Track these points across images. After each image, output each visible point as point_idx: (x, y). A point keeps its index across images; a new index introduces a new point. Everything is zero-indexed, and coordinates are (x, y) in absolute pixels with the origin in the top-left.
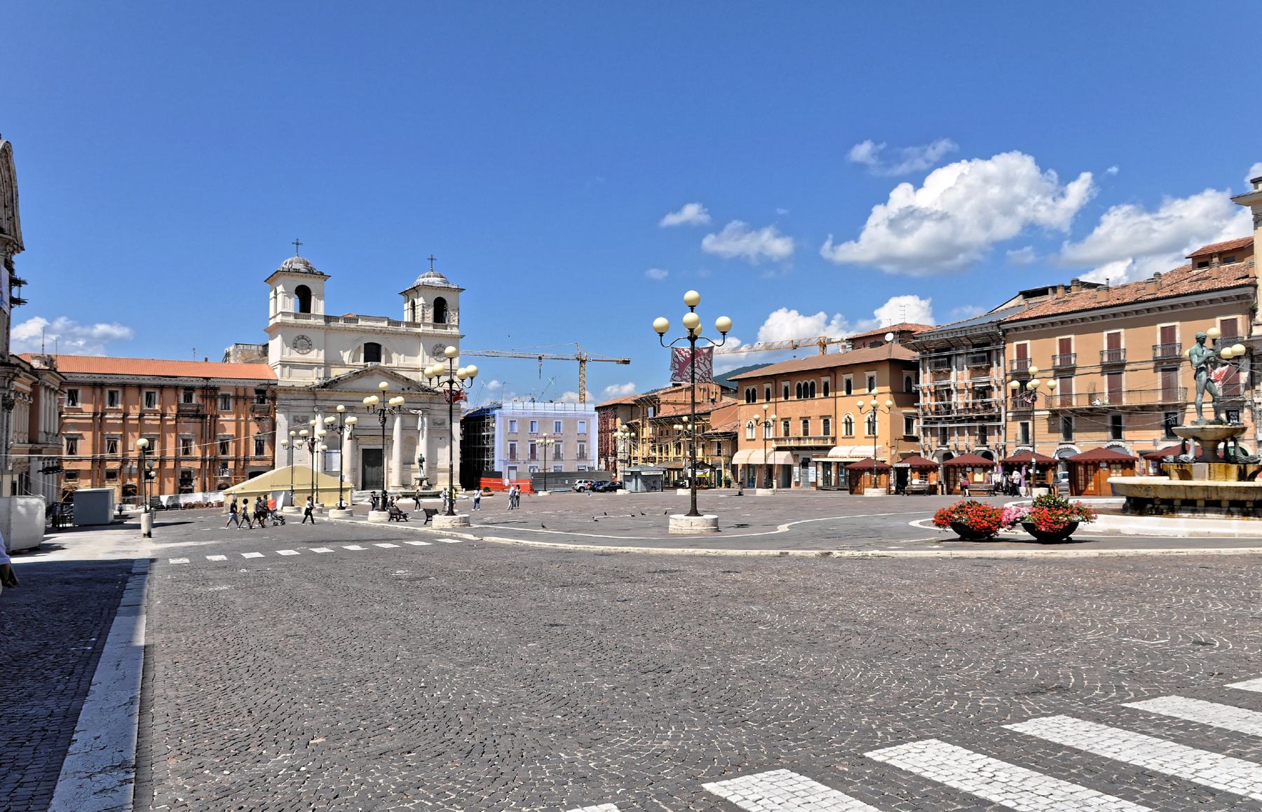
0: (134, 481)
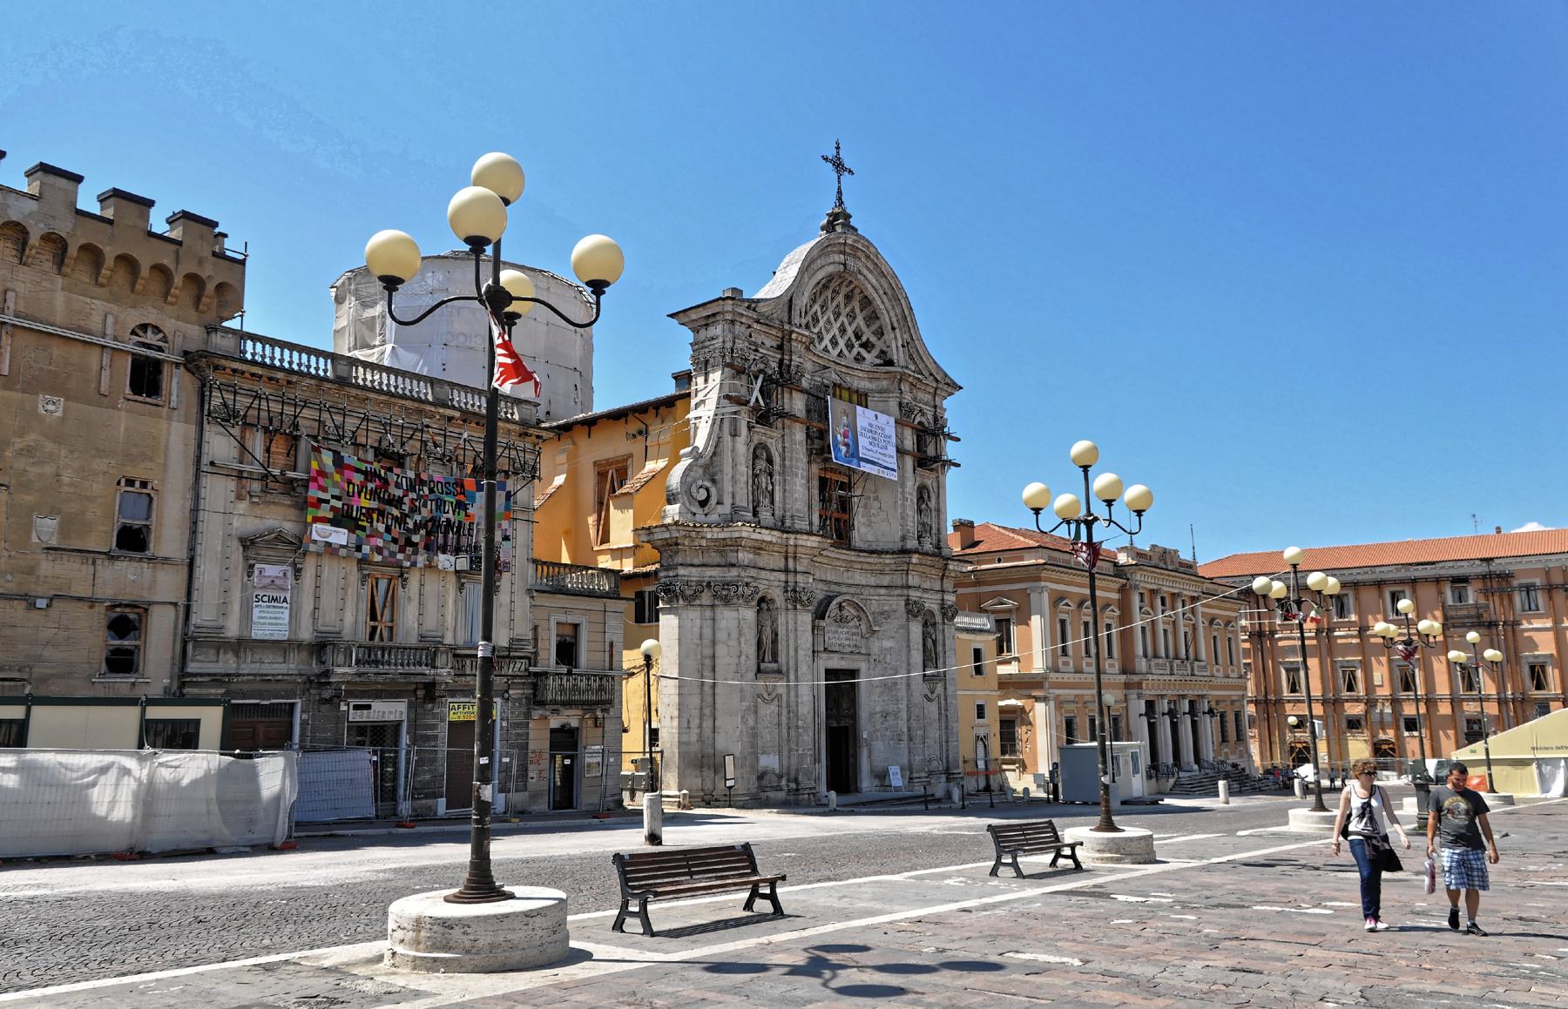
0: (1390, 734)
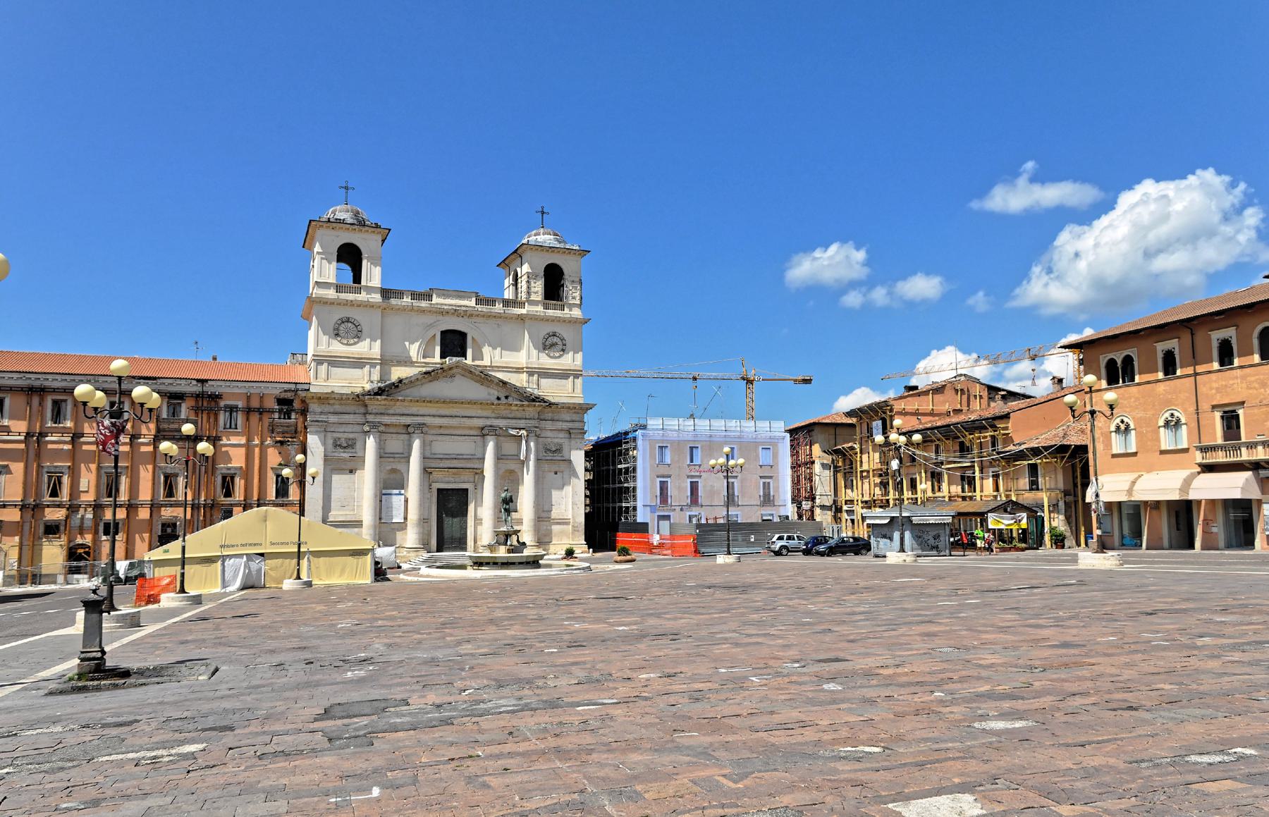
0: (88, 539)
